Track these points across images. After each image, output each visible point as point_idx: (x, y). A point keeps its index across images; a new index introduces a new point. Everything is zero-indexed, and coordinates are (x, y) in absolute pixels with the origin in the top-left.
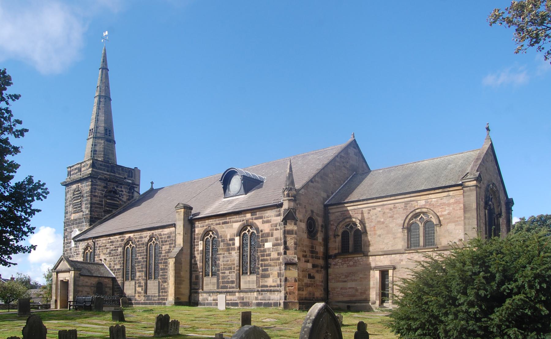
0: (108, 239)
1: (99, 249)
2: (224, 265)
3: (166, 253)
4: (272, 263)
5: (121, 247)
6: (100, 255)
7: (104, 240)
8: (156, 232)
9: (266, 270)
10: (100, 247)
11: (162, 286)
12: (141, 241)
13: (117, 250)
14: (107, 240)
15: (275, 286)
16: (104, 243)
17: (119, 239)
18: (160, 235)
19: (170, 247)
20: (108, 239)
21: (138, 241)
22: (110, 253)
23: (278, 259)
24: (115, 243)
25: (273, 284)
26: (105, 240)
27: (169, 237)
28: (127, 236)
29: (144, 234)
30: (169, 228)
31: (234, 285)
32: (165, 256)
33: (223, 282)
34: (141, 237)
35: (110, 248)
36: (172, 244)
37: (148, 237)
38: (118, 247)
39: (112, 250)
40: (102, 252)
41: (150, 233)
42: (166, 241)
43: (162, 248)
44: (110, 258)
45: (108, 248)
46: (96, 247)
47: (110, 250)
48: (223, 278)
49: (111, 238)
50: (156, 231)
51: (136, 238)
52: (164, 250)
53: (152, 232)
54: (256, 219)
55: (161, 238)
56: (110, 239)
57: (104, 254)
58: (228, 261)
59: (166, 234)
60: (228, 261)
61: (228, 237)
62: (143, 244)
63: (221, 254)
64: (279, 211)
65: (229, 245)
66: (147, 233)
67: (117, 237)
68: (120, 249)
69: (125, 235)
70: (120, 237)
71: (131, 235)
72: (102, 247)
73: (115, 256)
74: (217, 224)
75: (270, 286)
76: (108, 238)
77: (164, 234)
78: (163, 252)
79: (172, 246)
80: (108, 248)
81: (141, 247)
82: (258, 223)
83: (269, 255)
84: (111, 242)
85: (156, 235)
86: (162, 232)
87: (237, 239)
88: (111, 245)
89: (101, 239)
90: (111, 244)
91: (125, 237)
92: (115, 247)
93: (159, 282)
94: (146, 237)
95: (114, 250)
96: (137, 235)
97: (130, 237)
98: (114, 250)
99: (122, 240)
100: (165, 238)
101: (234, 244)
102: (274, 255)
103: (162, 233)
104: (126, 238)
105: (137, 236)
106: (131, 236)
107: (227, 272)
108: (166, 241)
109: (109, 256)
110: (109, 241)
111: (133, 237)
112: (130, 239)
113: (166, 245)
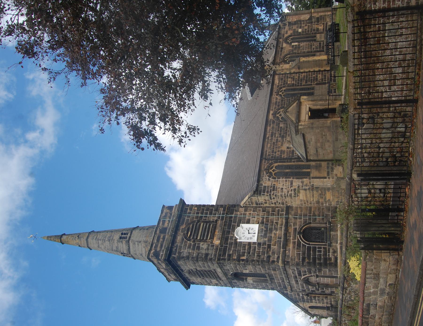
0: (268, 140)
1: (275, 153)
2: (308, 48)
3: (293, 80)
4: (310, 28)
5: (279, 124)
6: (282, 151)
7: (267, 146)
8: (275, 89)
9: (314, 30)
10: (273, 152)
11: (320, 81)
12: (279, 102)
13: (281, 127)
14: (268, 142)
15: (324, 26)
16: (271, 146)
17: (271, 126)
18: (278, 86)
19: (290, 78)
20: (268, 140)
21: (279, 106)
22: (283, 137)
23: (309, 26)
24: (274, 131)
25: (322, 26)
26: (268, 144)
27: (282, 79)
28: (271, 117)
29: (274, 100)
30: (275, 79)
31: (322, 43)
32: (296, 81)
33: (320, 48)
34: (276, 102)
35: (277, 137)
36: (288, 76)
37: (277, 97)
38: (279, 126)
39: (280, 134)
40: (279, 147)
41: (275, 95)
42: (285, 81)
43: (289, 84)
44: (287, 136)
45: (277, 140)
46: (272, 157)
47: (280, 137)
48: (317, 48)
49: (267, 136)
50: (274, 90)
51: (275, 108)
52: (291, 82)
53: (274, 93)
54: (284, 36)
55: (281, 85)
56: (268, 138)
57: (282, 145)
58: (306, 47)
59: (279, 82)
60: (306, 47)
61: (291, 48)
62: (282, 101)
63: (301, 51)
64: (283, 28)
65: (296, 48)
66: (274, 97)
67: (268, 128)
68: (282, 124)
69: (269, 120)
70: (270, 124)
71: (271, 112)
72: (273, 148)
73: (286, 130)
74: (281, 55)
75: (324, 27)
76: (267, 140)
77: (279, 83)
78: (293, 83)
79: (289, 76)
80: (277, 140)
81: (285, 102)
82: (286, 36)
83: (306, 29)
84: (272, 136)
85: (277, 90)
86: (276, 85)
87: (293, 44)
88: (275, 137)
89: (265, 149)
90: (274, 136)
91: (271, 119)
92: (278, 130)
93: (317, 84)
94: (277, 98)
95: (281, 132)
96: (273, 107)
97: (272, 114)
98: (281, 132)
99: (274, 122)
100: (282, 82)
101: (296, 45)
102: (306, 27)
103: (277, 85)
104: (272, 118)
105: (274, 107)
106: (272, 113)
107: (313, 47)
108: (285, 81)
109: (286, 137)
110: (270, 138)
111: (273, 111)
112: (274, 114)
113: (287, 81)
